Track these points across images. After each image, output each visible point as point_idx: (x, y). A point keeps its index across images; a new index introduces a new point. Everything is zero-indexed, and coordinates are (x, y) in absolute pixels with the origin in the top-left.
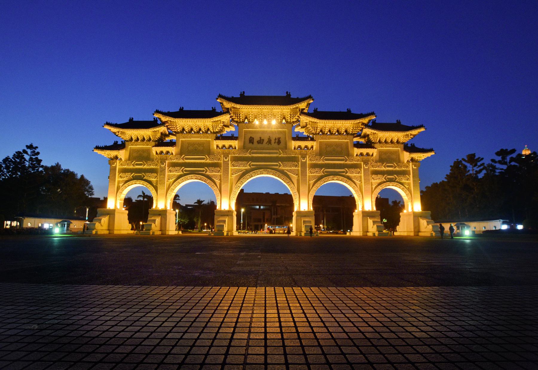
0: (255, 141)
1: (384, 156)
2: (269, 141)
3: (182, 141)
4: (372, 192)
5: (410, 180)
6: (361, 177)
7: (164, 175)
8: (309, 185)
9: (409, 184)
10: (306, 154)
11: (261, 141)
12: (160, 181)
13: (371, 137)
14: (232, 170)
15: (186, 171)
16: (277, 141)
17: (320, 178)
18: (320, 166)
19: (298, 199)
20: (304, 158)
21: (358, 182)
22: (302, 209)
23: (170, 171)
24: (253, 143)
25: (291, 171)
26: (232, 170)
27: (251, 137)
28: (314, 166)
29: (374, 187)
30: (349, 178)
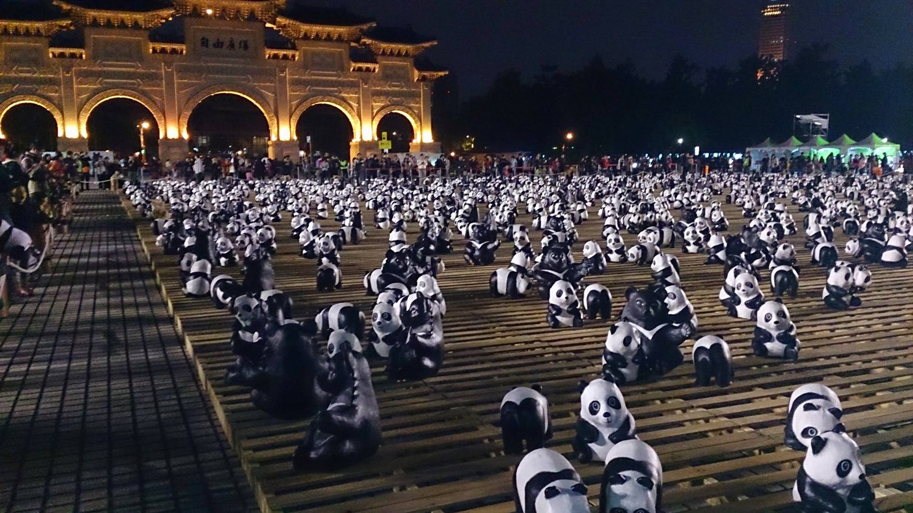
0: (211, 43)
1: (389, 72)
2: (232, 45)
3: (94, 38)
4: (373, 119)
5: (421, 105)
6: (359, 98)
7: (72, 88)
8: (291, 108)
9: (419, 108)
10: (285, 67)
11: (219, 44)
12: (66, 97)
13: (373, 47)
14: (179, 83)
15: (106, 83)
16: (243, 44)
17: (305, 99)
18: (305, 83)
19: (275, 125)
20: (282, 72)
21: (355, 105)
22: (282, 138)
23: (80, 83)
24: (207, 46)
25: (266, 88)
26: (179, 83)
27: (203, 39)
28: (296, 83)
29: (375, 111)
30: (344, 100)
